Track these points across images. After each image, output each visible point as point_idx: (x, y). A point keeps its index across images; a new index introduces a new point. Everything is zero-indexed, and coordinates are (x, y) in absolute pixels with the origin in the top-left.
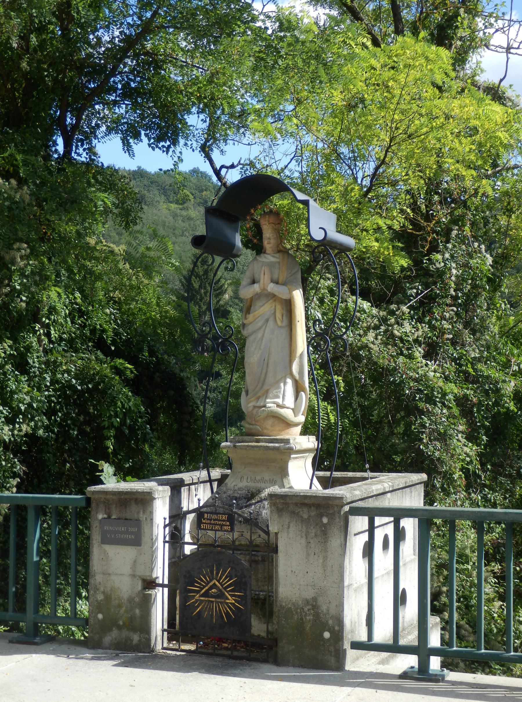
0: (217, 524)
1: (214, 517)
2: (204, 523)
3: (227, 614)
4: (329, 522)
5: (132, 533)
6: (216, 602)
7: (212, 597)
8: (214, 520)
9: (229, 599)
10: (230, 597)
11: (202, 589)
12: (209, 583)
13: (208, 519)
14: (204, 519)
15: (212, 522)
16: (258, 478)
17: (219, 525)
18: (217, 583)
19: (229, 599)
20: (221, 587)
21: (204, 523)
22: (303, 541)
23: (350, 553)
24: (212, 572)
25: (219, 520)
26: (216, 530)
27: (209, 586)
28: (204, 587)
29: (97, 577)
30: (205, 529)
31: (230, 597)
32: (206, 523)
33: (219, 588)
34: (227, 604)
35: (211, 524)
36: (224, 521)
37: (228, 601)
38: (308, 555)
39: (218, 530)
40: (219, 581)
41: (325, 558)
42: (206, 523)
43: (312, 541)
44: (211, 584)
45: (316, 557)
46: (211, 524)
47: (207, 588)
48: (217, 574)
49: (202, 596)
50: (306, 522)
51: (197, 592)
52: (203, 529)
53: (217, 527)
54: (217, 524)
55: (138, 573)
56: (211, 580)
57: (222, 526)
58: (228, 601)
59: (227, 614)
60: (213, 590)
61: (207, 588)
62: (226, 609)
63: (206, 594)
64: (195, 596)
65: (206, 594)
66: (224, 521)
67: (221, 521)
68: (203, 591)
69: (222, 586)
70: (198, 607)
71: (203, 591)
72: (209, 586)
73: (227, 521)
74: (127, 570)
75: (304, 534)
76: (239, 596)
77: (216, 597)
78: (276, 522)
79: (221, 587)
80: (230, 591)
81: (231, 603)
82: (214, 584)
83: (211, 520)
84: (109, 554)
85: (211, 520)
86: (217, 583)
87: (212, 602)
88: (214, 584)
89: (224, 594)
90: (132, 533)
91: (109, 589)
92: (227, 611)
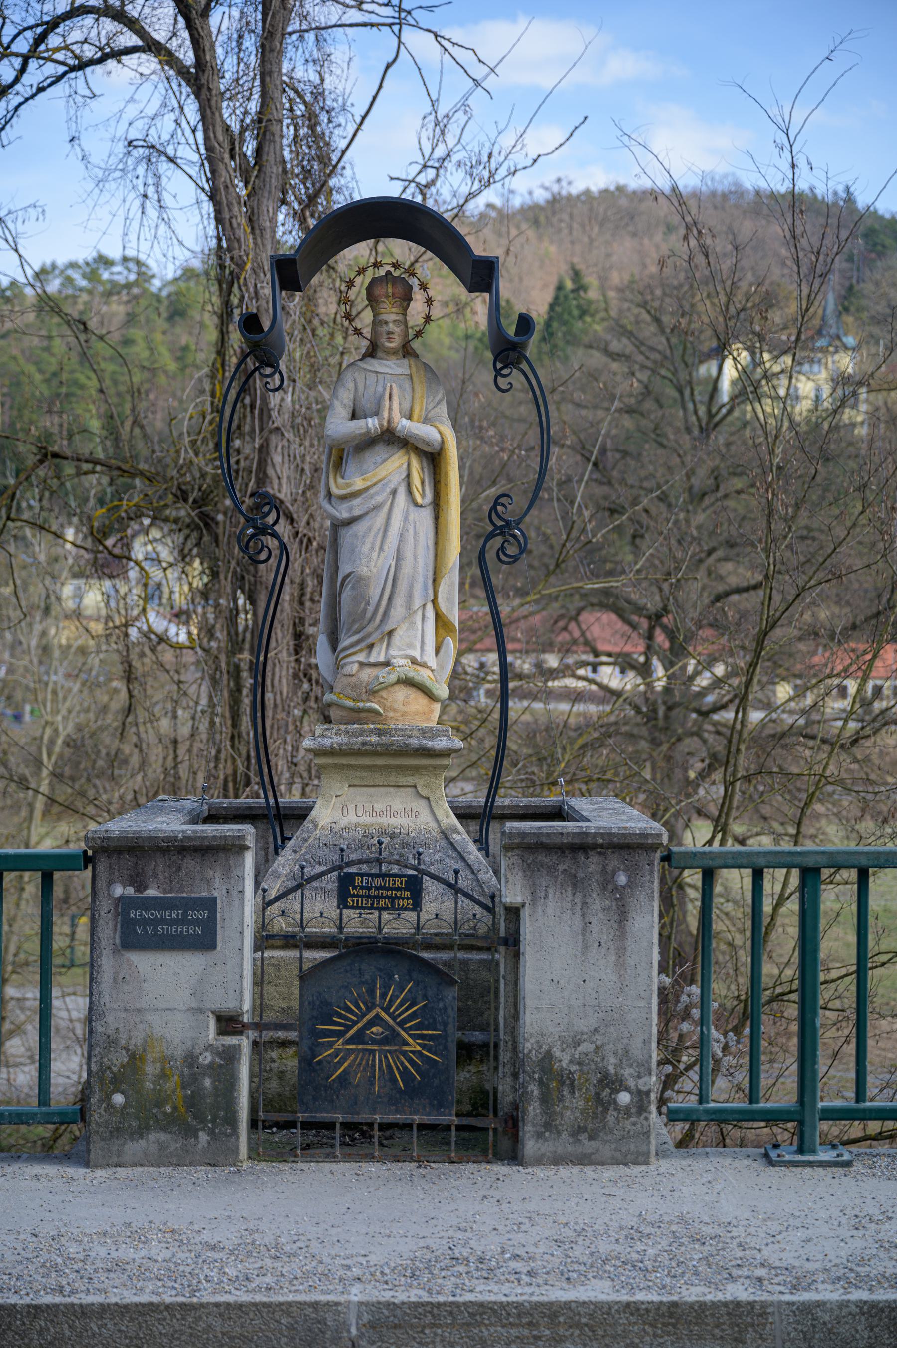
0: (382, 897)
1: (378, 881)
2: (354, 895)
3: (405, 1073)
4: (630, 884)
5: (196, 923)
6: (380, 1051)
7: (374, 1042)
8: (377, 888)
9: (408, 1044)
10: (410, 1040)
11: (349, 1028)
12: (364, 1015)
13: (362, 888)
14: (355, 887)
15: (373, 892)
16: (378, 807)
17: (387, 897)
18: (383, 1014)
19: (408, 1044)
20: (391, 1022)
21: (354, 895)
22: (577, 922)
23: (396, 944)
24: (371, 992)
25: (388, 889)
26: (381, 910)
27: (365, 1020)
28: (355, 1023)
29: (110, 1018)
30: (358, 908)
31: (410, 1040)
32: (358, 896)
33: (386, 1022)
34: (404, 1054)
35: (369, 896)
36: (398, 889)
37: (406, 1048)
38: (586, 948)
39: (386, 909)
40: (386, 1010)
41: (621, 952)
42: (358, 896)
43: (594, 920)
44: (368, 1017)
45: (603, 950)
46: (369, 896)
47: (360, 1025)
48: (383, 995)
49: (350, 1041)
50: (576, 883)
51: (340, 1034)
52: (352, 908)
53: (382, 903)
54: (382, 897)
55: (208, 1005)
56: (369, 1009)
57: (393, 899)
58: (406, 1048)
59: (405, 1073)
60: (374, 1029)
61: (360, 1025)
62: (402, 1064)
63: (358, 1038)
64: (334, 1042)
65: (358, 1038)
66: (398, 889)
67: (392, 889)
68: (352, 1032)
69: (394, 1019)
70: (340, 1064)
71: (352, 1032)
72: (365, 1020)
73: (406, 889)
74: (183, 999)
75: (578, 908)
76: (430, 1037)
77: (385, 1041)
78: (519, 887)
79: (391, 1022)
80: (410, 1028)
81: (413, 1052)
82: (377, 1016)
83: (369, 888)
84: (140, 969)
85: (369, 888)
86: (383, 1014)
87: (373, 1052)
88: (377, 1016)
89: (398, 1034)
90: (196, 923)
91: (139, 1041)
92: (405, 1068)
